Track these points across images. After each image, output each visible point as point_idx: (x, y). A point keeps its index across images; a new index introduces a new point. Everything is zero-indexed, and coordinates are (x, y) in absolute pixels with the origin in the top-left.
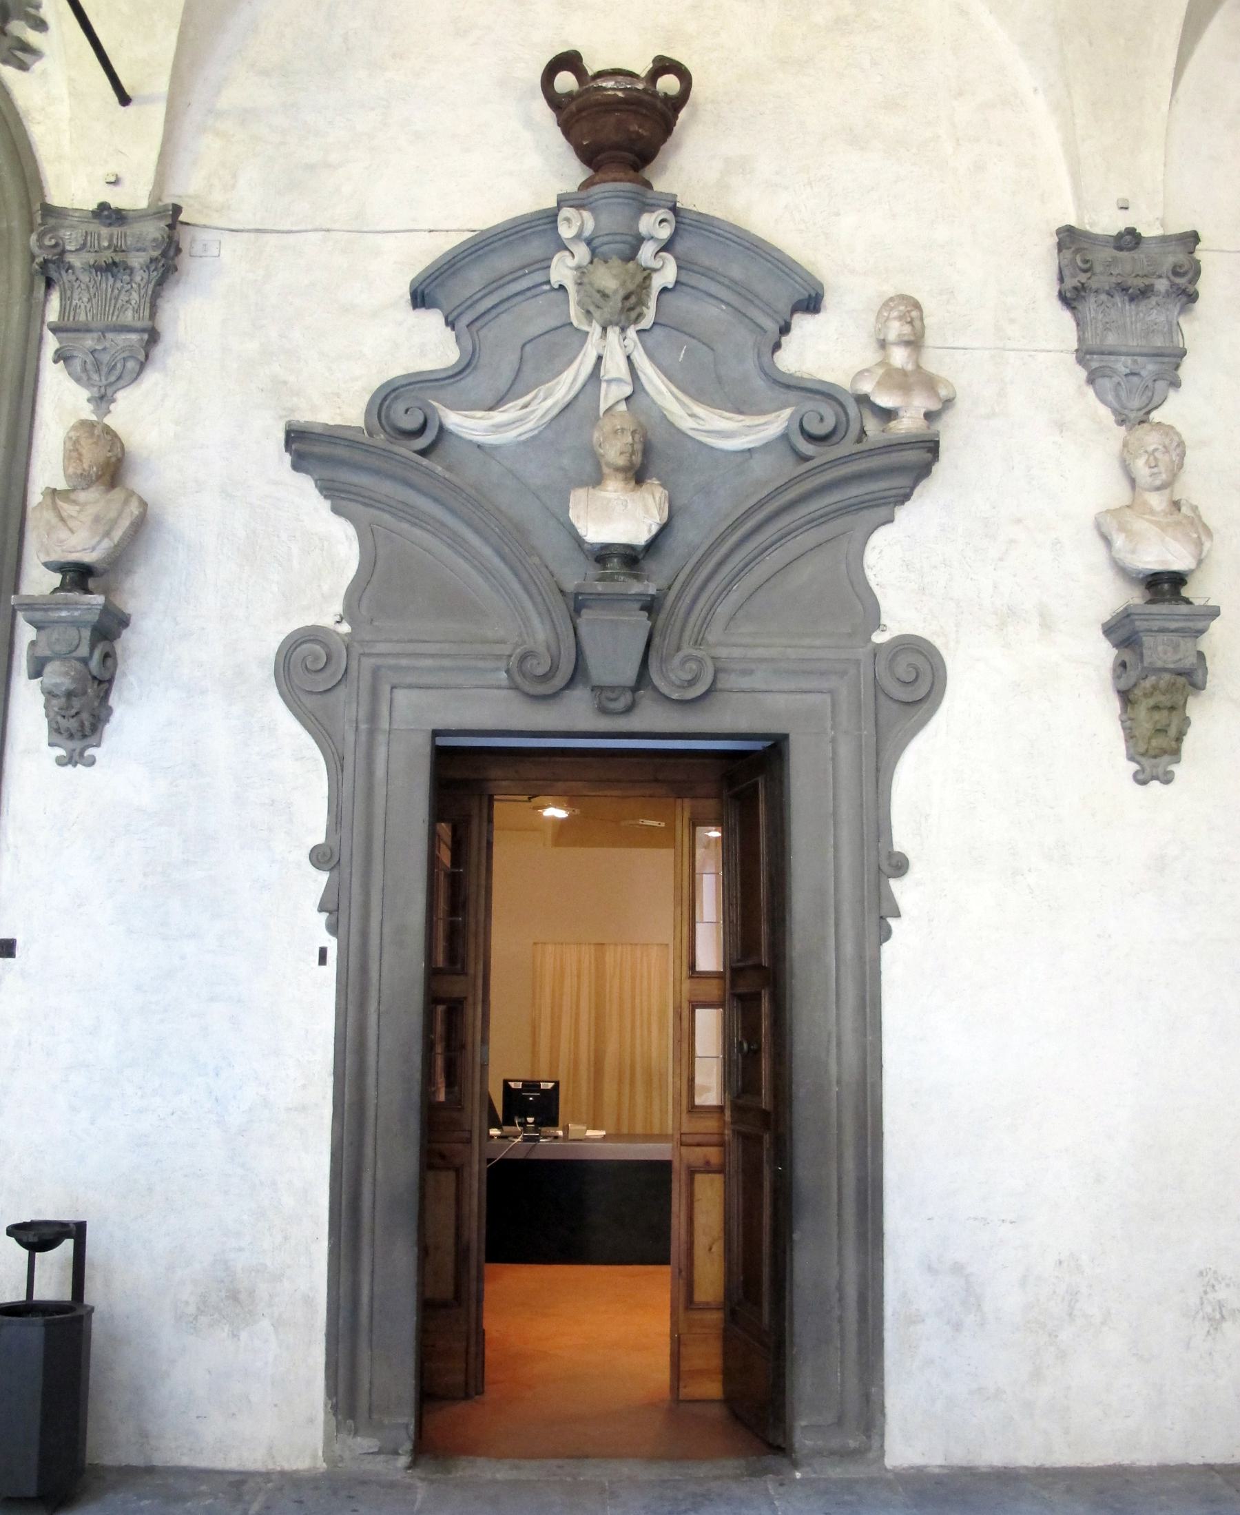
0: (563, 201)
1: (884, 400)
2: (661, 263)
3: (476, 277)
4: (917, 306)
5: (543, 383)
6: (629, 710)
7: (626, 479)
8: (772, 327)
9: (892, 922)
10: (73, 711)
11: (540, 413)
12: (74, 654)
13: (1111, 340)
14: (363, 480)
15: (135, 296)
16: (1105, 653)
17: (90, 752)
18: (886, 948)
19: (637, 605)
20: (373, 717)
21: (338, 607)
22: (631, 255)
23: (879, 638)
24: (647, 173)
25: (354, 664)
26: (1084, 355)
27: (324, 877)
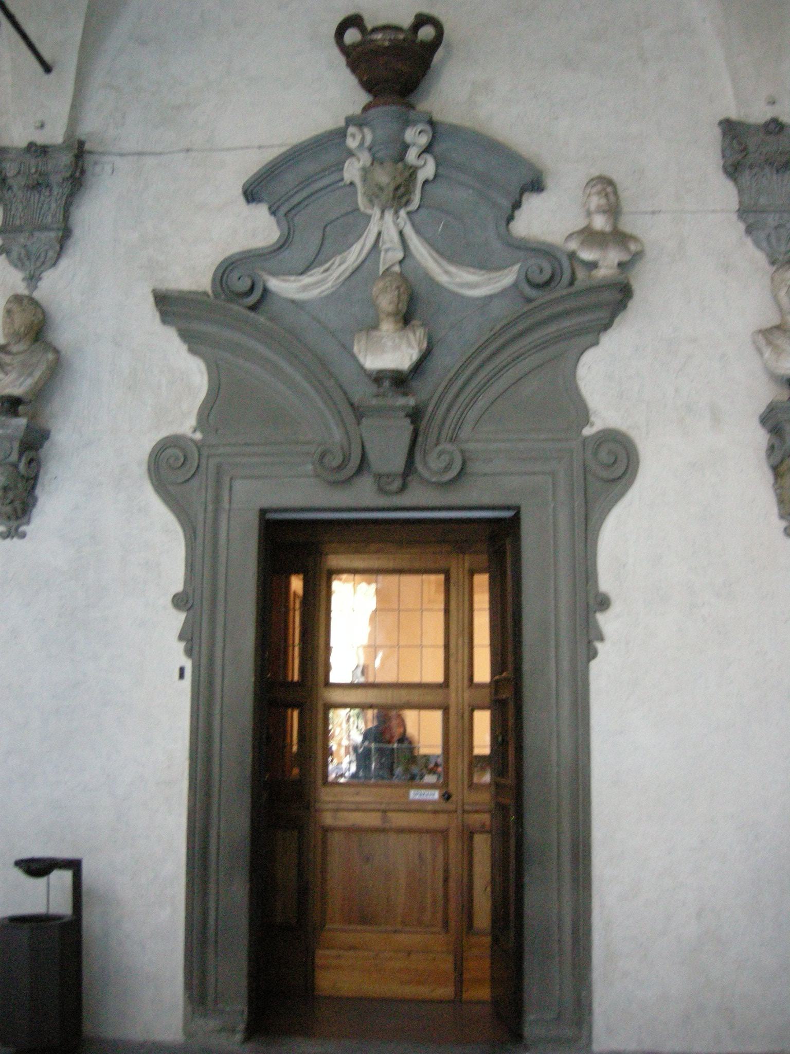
0: (349, 121)
1: (587, 255)
2: (423, 163)
3: (290, 178)
4: (610, 182)
5: (340, 253)
6: (403, 488)
7: (396, 322)
8: (506, 203)
9: (599, 645)
10: (8, 501)
11: (336, 275)
12: (7, 460)
13: (762, 201)
14: (211, 329)
15: (53, 206)
16: (761, 437)
17: (23, 528)
18: (594, 665)
19: (403, 414)
20: (217, 499)
21: (192, 421)
22: (401, 157)
23: (587, 431)
24: (412, 99)
25: (204, 461)
26: (743, 212)
27: (182, 617)
